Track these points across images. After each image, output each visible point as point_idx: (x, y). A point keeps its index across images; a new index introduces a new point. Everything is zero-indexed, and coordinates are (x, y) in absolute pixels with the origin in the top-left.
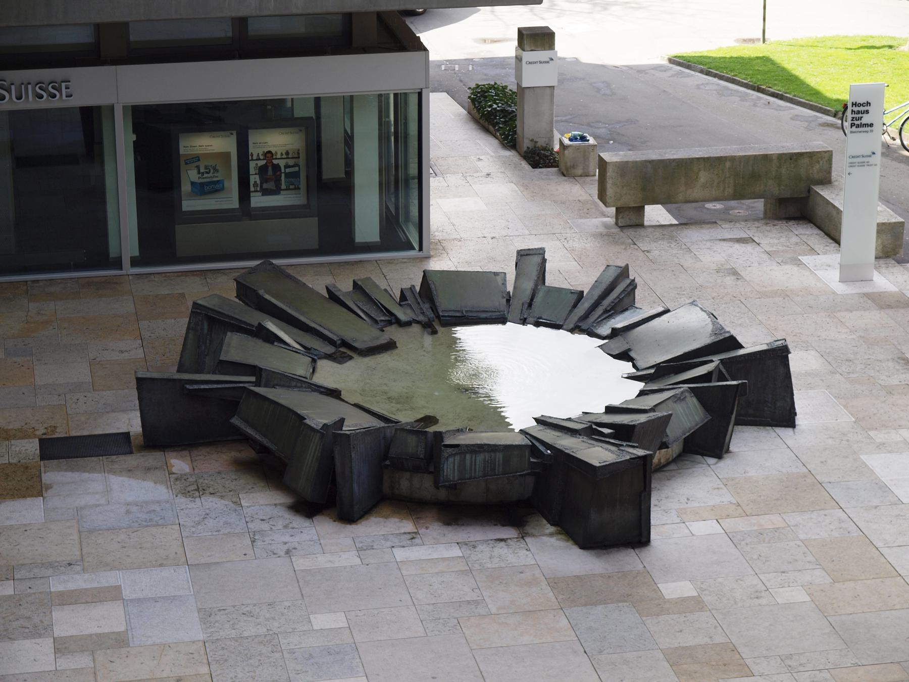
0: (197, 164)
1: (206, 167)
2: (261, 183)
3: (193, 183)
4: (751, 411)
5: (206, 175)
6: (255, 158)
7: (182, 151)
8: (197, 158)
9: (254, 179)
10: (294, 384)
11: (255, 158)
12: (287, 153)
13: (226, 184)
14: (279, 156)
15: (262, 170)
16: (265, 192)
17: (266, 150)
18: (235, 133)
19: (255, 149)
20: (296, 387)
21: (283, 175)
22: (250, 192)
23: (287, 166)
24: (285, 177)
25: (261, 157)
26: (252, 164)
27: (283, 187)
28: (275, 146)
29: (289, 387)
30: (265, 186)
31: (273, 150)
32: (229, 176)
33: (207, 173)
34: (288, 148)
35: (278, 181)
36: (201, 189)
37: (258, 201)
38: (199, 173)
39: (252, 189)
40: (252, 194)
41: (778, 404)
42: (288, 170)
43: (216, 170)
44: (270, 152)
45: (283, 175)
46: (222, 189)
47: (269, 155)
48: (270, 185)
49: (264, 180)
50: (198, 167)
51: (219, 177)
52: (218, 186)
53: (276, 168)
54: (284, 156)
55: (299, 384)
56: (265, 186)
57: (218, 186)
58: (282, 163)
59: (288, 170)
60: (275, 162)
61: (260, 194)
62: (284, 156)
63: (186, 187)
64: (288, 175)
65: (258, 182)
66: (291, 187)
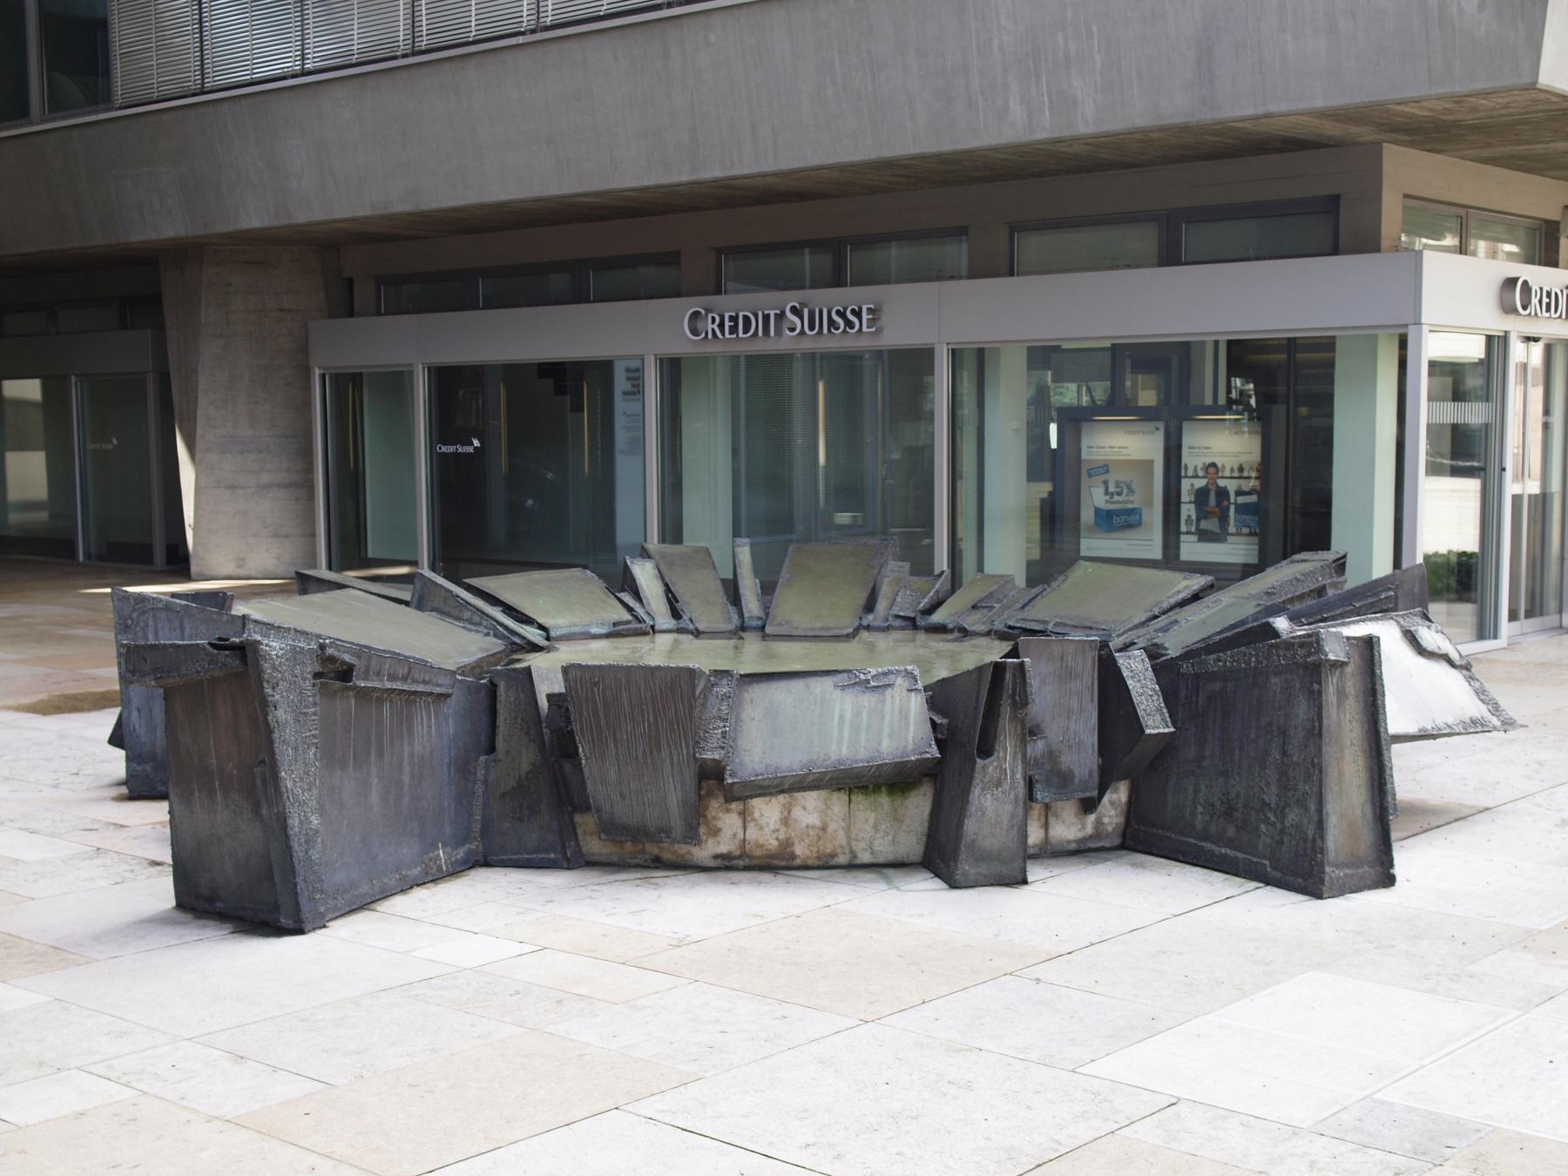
0: (1103, 478)
1: (1117, 485)
2: (1198, 520)
3: (1097, 511)
4: (1231, 831)
5: (1116, 498)
6: (1190, 473)
7: (1084, 456)
8: (1105, 468)
9: (1188, 510)
10: (467, 615)
11: (1190, 473)
12: (1241, 469)
13: (1145, 517)
14: (1227, 474)
15: (1201, 496)
16: (1204, 536)
17: (1208, 461)
18: (1161, 425)
19: (1192, 460)
20: (470, 621)
21: (1232, 508)
22: (1179, 533)
23: (1239, 493)
24: (1237, 511)
25: (1201, 473)
26: (1186, 485)
27: (1232, 529)
28: (1223, 454)
29: (458, 619)
30: (1204, 525)
31: (1219, 462)
32: (1150, 504)
33: (1119, 494)
34: (1244, 459)
35: (1224, 519)
36: (1111, 521)
37: (1191, 549)
38: (1107, 493)
39: (1183, 528)
40: (1183, 538)
41: (1292, 817)
42: (1241, 500)
43: (1131, 491)
44: (1213, 465)
45: (1232, 508)
46: (1139, 524)
47: (1212, 470)
48: (1211, 525)
49: (1203, 514)
50: (1106, 483)
51: (1135, 501)
52: (1133, 519)
53: (1222, 494)
54: (1236, 474)
55: (477, 619)
56: (1204, 525)
57: (1133, 519)
58: (1232, 486)
59: (1241, 500)
60: (1221, 483)
61: (1194, 538)
62: (1236, 474)
63: (1087, 516)
64: (1241, 509)
65: (1194, 517)
66: (1246, 530)
